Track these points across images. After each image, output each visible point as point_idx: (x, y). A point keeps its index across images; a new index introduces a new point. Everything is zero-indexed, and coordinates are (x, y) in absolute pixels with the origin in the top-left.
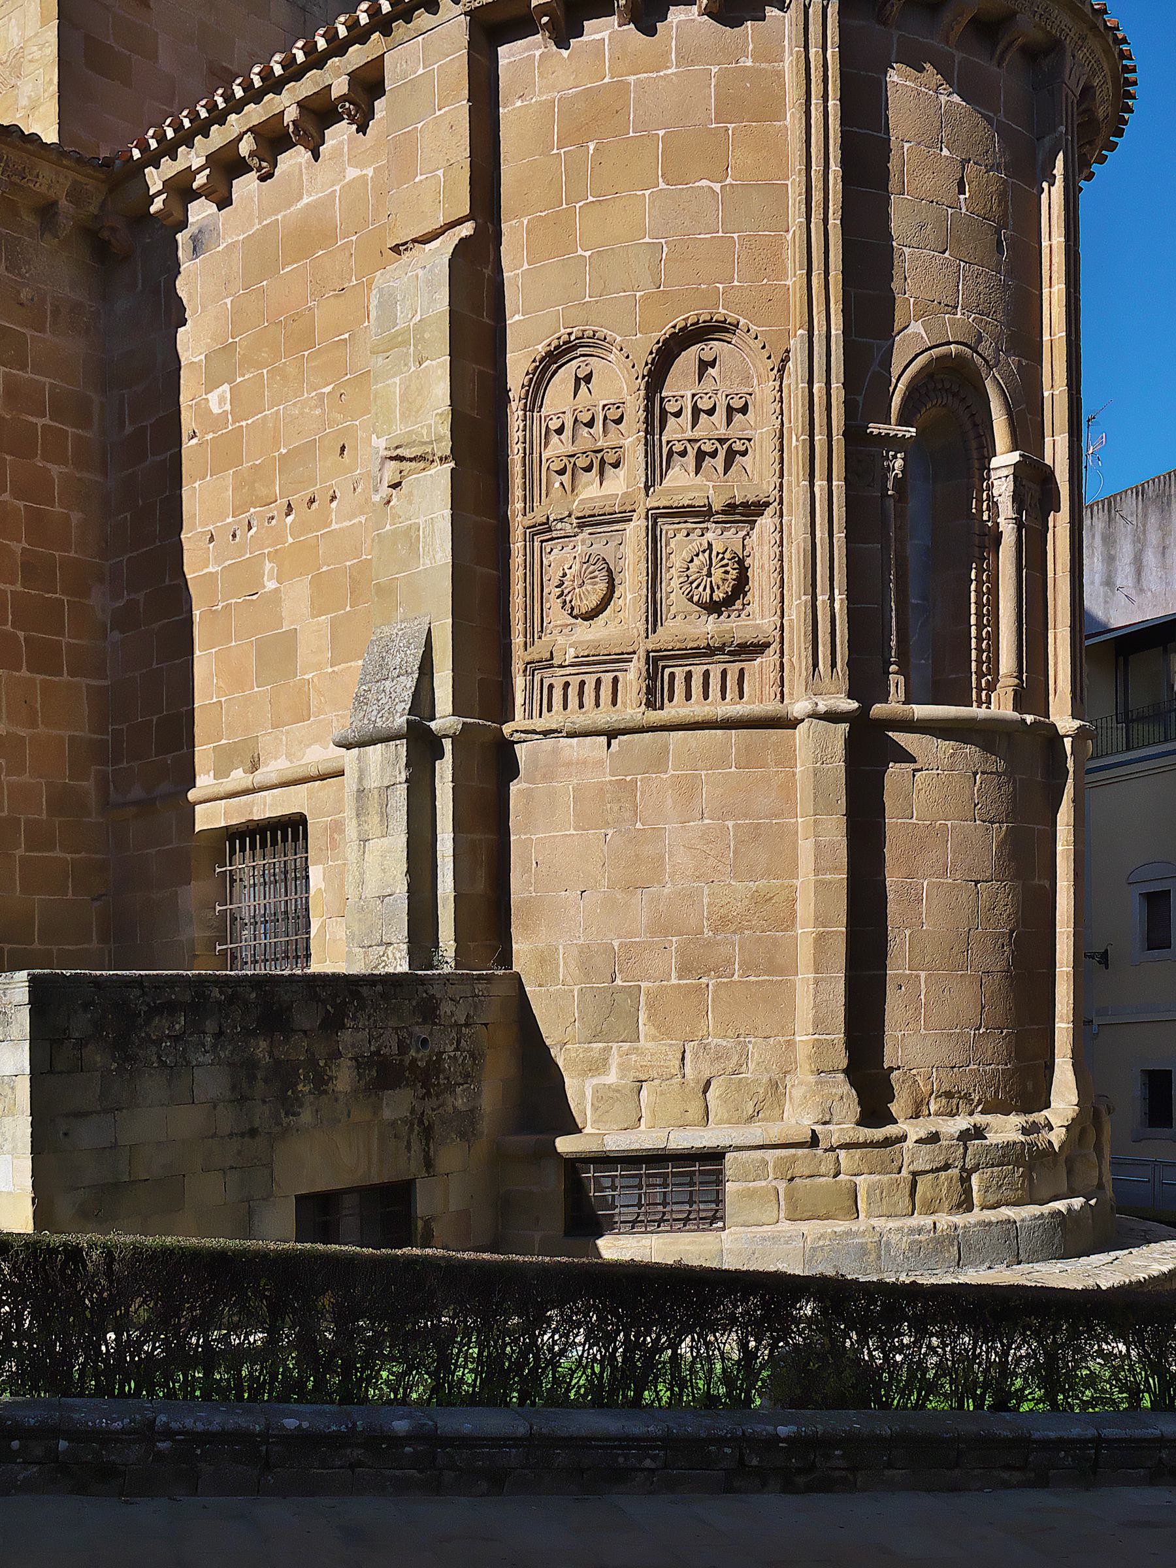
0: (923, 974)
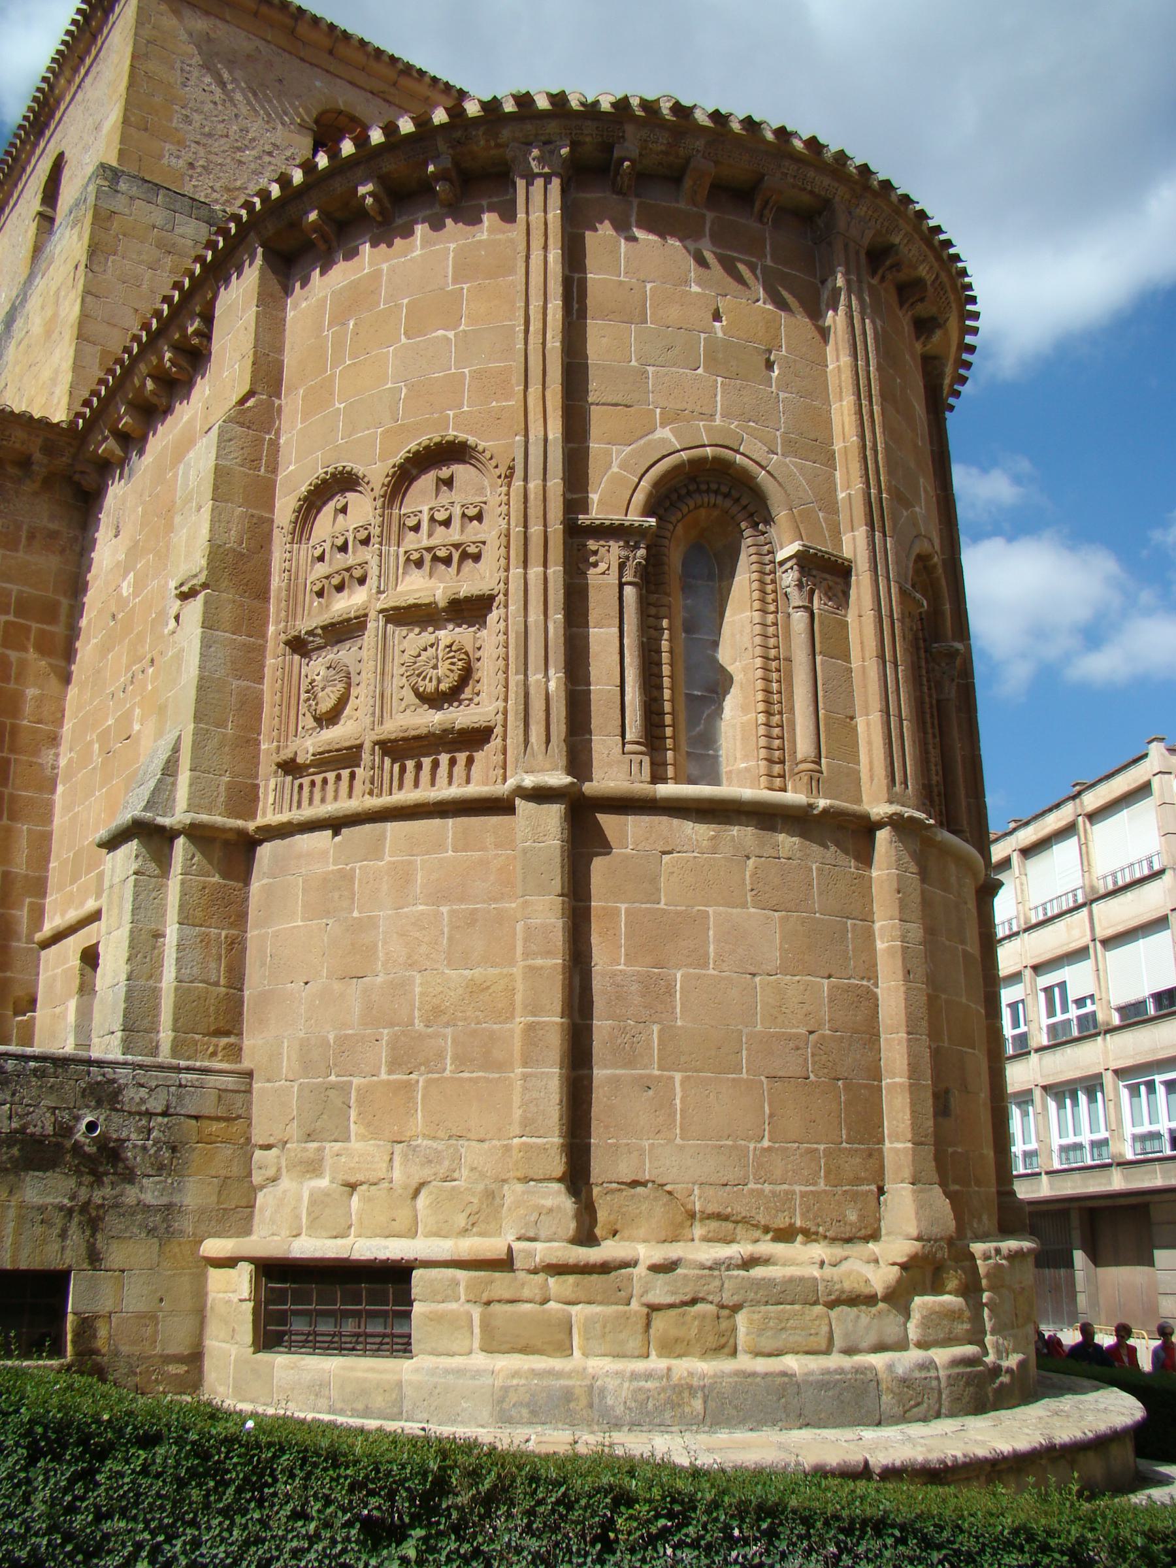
0: (678, 1076)
